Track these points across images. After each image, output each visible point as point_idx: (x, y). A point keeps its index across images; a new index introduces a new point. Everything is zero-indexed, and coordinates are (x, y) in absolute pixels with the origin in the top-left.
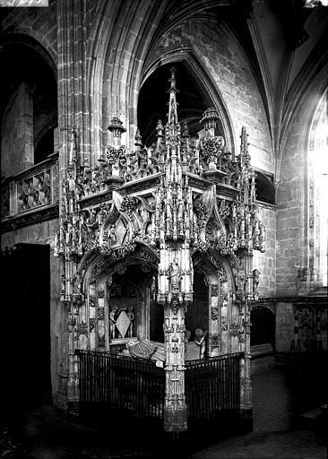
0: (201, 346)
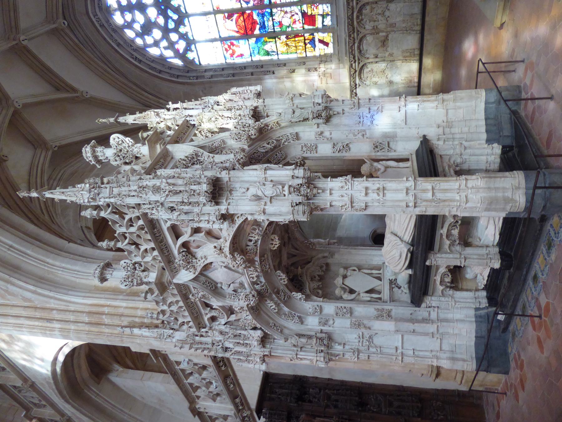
0: (387, 167)
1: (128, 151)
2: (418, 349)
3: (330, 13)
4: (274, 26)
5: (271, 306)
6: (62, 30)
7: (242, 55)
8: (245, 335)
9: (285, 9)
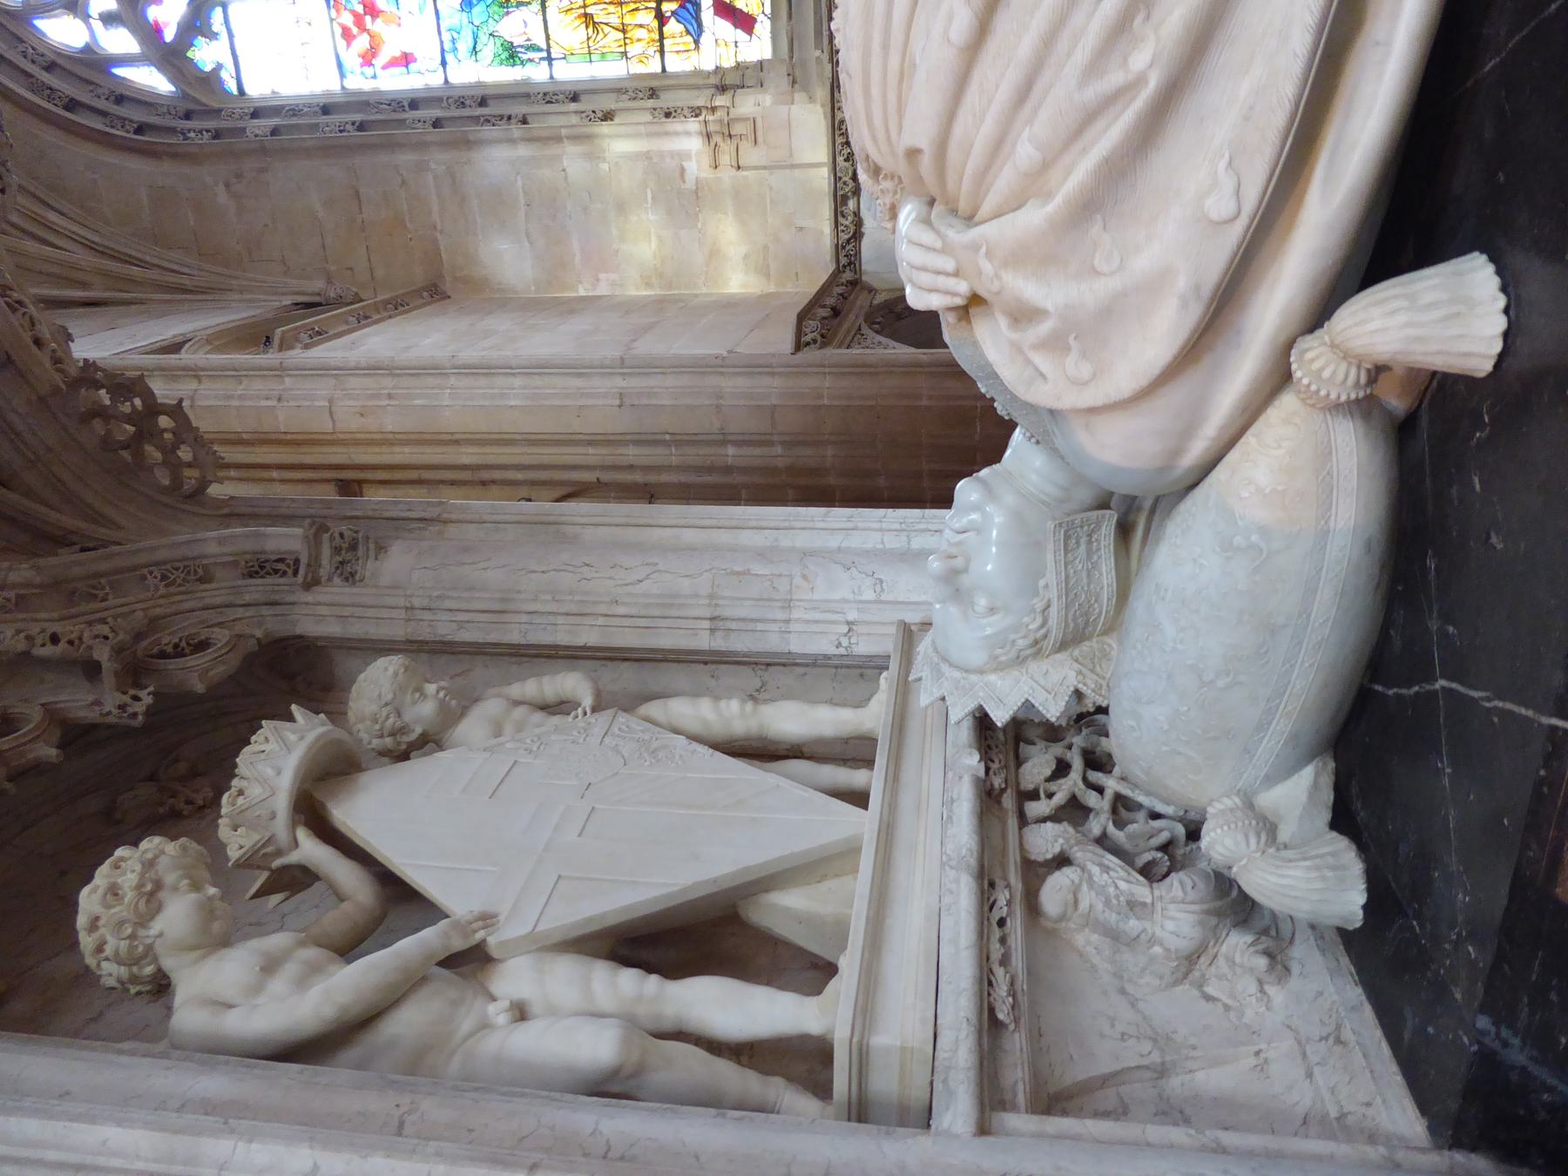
7: (406, 60)
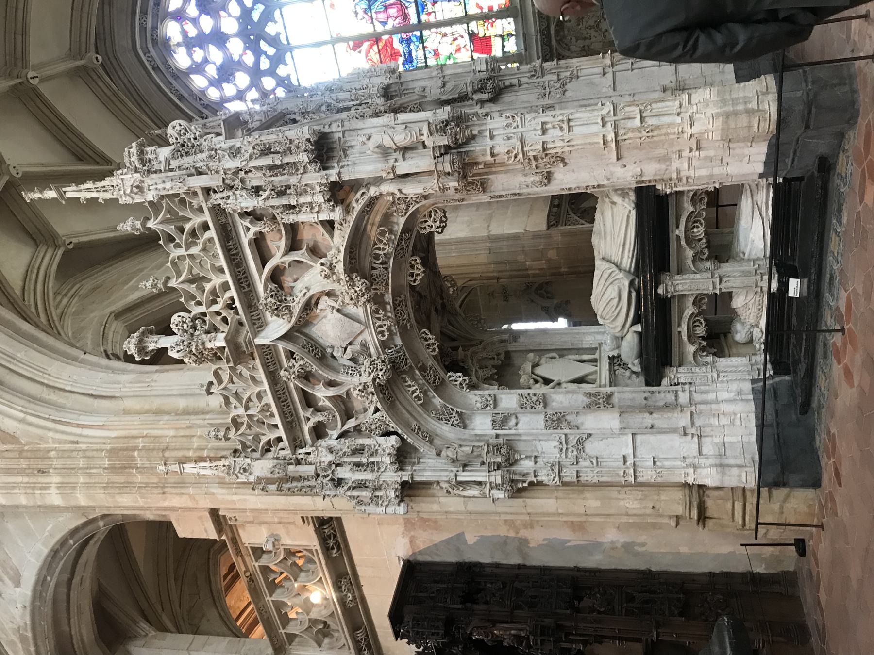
1: (193, 146)
2: (661, 456)
3: (514, 33)
4: (426, 58)
5: (413, 392)
6: (94, 70)
8: (370, 447)
9: (444, 30)
